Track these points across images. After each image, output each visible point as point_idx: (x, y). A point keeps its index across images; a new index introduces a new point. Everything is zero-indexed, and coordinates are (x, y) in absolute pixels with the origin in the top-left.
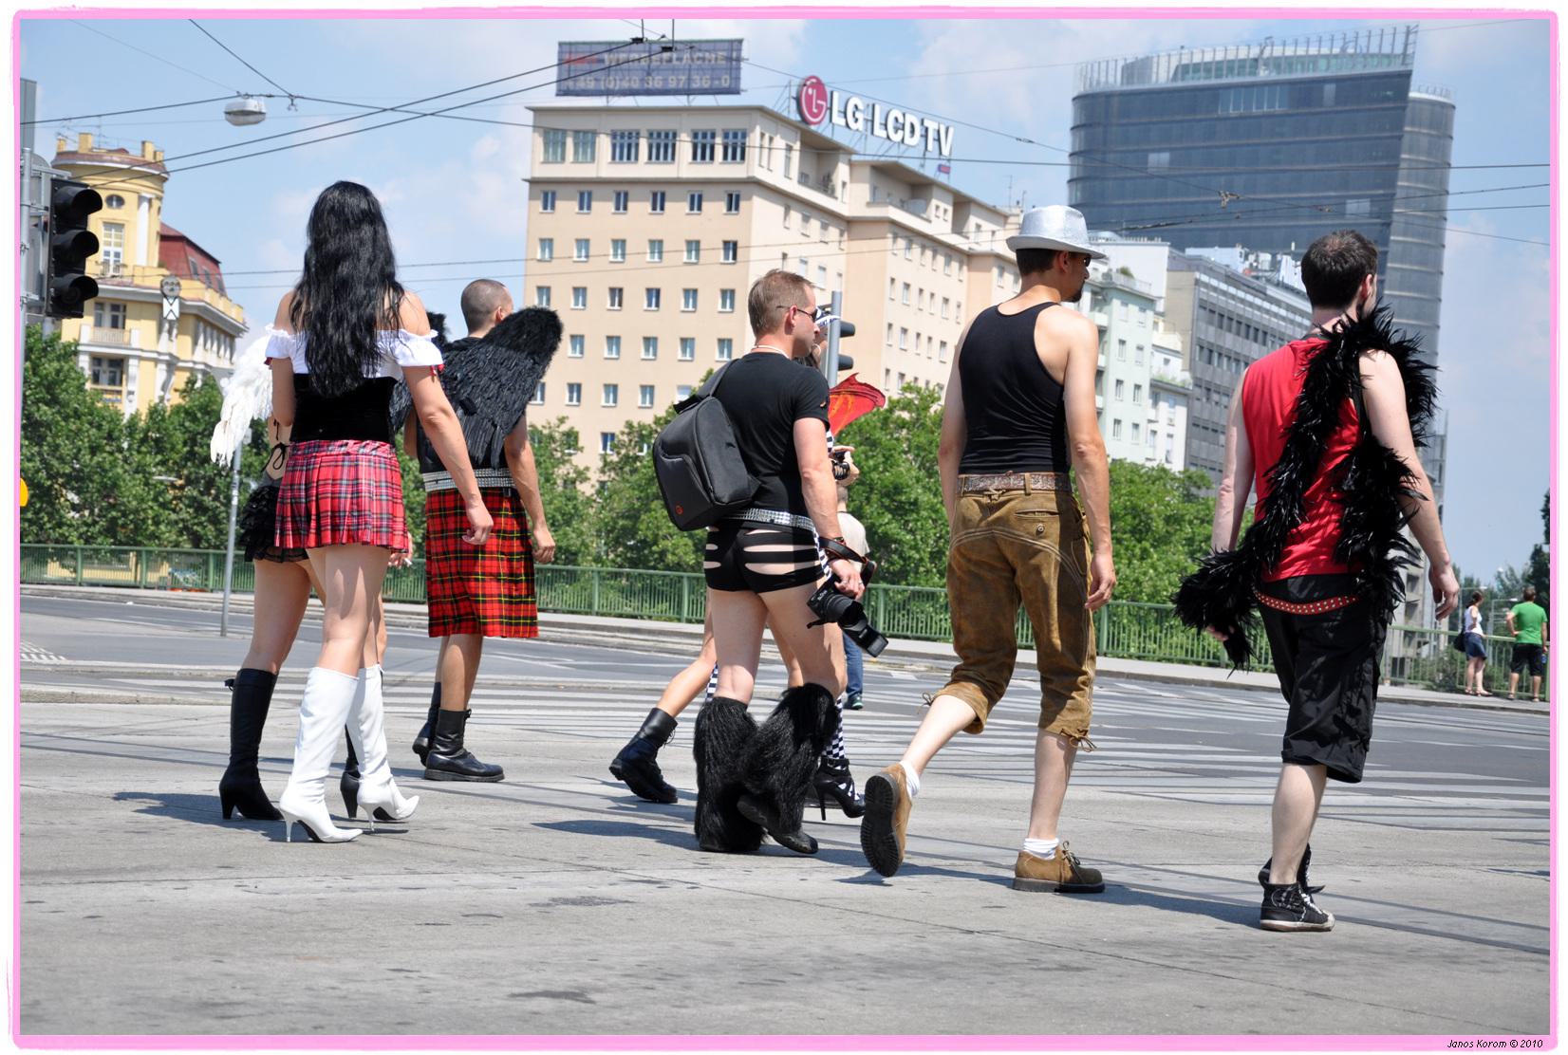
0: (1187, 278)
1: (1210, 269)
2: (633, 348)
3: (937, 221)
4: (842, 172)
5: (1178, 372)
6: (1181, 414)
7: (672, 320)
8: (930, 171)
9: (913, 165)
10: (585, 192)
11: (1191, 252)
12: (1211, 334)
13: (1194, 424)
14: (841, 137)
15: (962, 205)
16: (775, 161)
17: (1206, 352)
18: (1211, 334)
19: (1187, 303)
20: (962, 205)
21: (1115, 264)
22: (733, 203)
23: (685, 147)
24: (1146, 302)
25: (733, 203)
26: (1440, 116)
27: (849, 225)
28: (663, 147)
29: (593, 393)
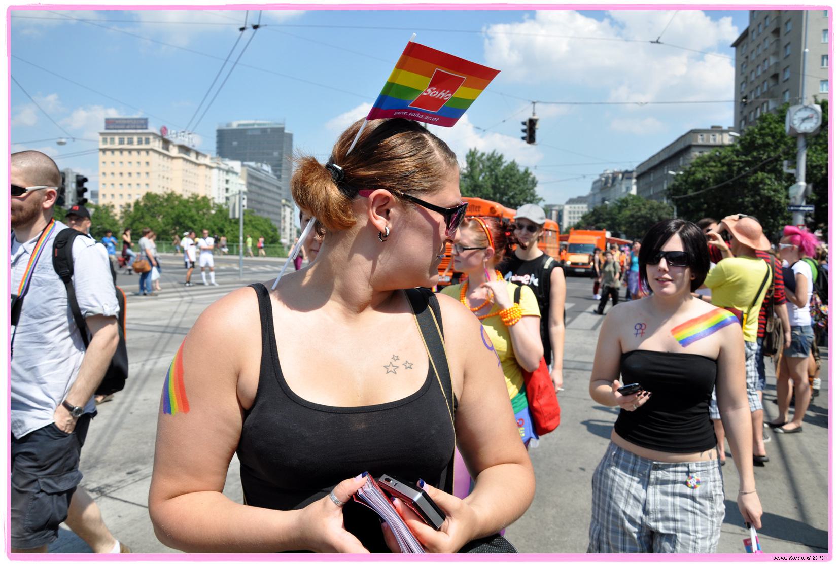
0: (245, 169)
1: (249, 166)
2: (126, 186)
3: (192, 157)
4: (171, 146)
7: (134, 179)
8: (190, 146)
10: (113, 151)
11: (245, 163)
12: (250, 180)
14: (171, 139)
15: (198, 154)
16: (157, 145)
17: (249, 184)
18: (250, 180)
19: (245, 175)
20: (198, 154)
22: (147, 153)
24: (237, 174)
25: (147, 153)
26: (290, 136)
27: (173, 158)
28: (131, 142)
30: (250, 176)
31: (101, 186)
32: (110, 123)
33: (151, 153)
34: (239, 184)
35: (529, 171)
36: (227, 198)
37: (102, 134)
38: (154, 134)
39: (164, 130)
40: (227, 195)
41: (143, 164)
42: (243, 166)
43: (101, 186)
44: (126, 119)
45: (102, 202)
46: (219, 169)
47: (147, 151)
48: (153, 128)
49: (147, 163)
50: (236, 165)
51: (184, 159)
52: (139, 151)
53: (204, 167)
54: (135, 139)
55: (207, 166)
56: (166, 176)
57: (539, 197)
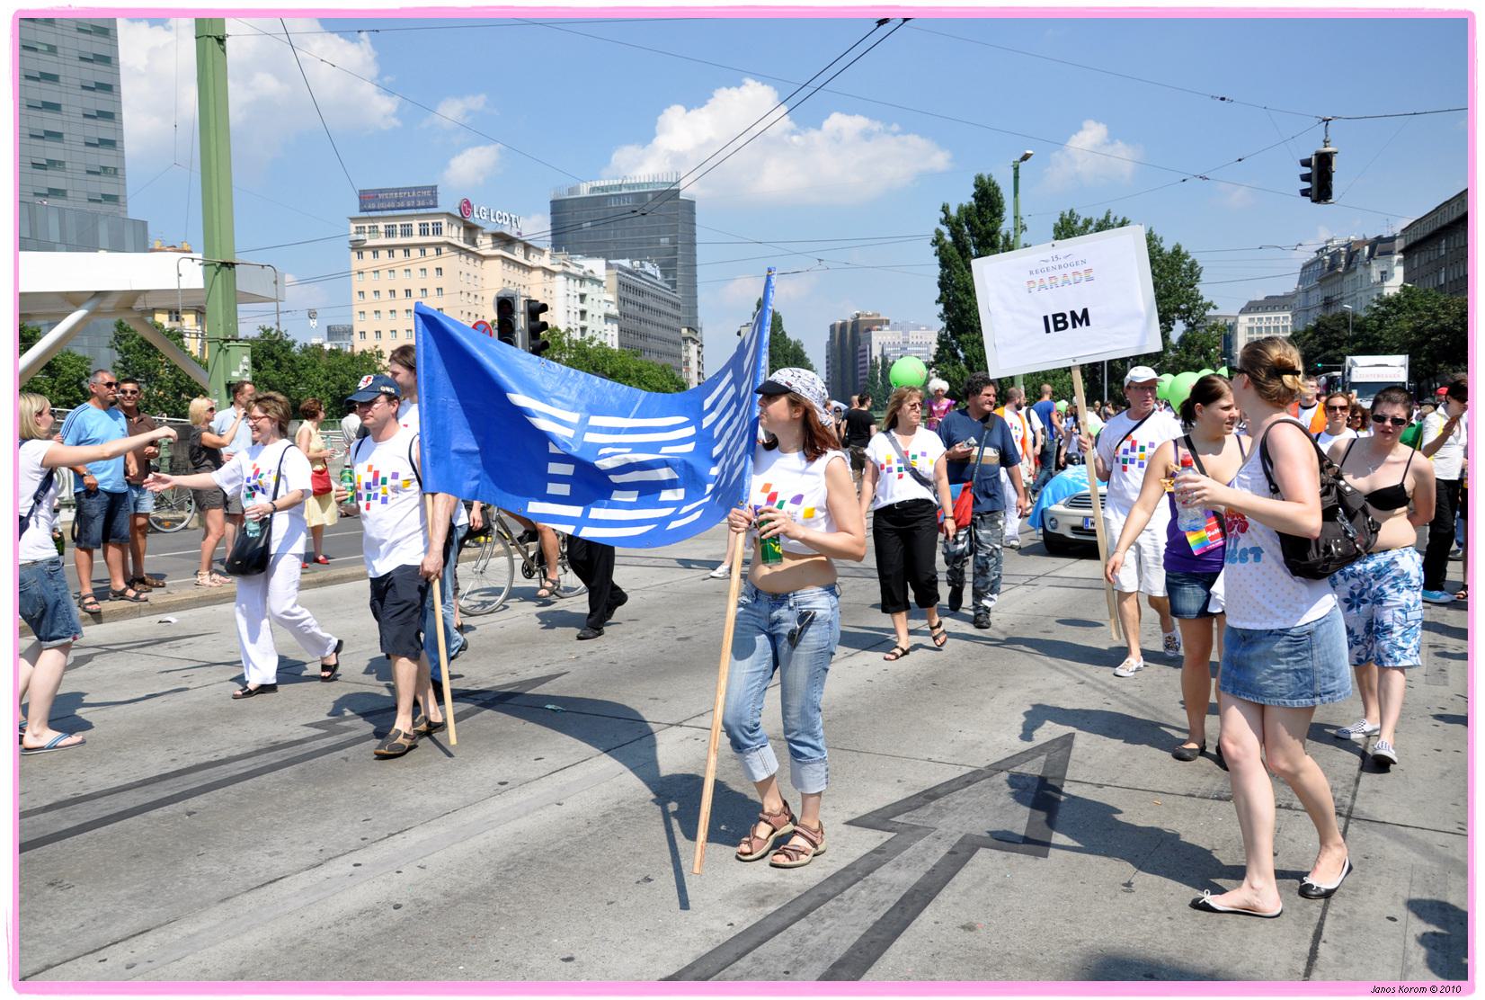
1: (621, 268)
3: (519, 255)
5: (614, 311)
6: (616, 327)
8: (514, 235)
9: (507, 231)
12: (624, 294)
13: (621, 330)
14: (478, 223)
16: (454, 234)
17: (622, 301)
18: (624, 294)
21: (586, 269)
22: (439, 252)
23: (416, 229)
24: (600, 283)
25: (439, 252)
27: (485, 258)
28: (407, 232)
29: (386, 334)
30: (623, 285)
31: (357, 317)
32: (372, 202)
33: (444, 249)
34: (604, 300)
35: (1183, 251)
36: (583, 329)
37: (353, 220)
38: (449, 214)
39: (466, 206)
40: (583, 323)
41: (432, 272)
42: (609, 266)
43: (357, 317)
44: (398, 190)
45: (360, 346)
46: (568, 275)
47: (438, 247)
48: (448, 203)
49: (439, 270)
50: (597, 266)
51: (503, 258)
52: (422, 247)
53: (540, 273)
54: (416, 229)
55: (545, 270)
56: (471, 288)
57: (1206, 300)
